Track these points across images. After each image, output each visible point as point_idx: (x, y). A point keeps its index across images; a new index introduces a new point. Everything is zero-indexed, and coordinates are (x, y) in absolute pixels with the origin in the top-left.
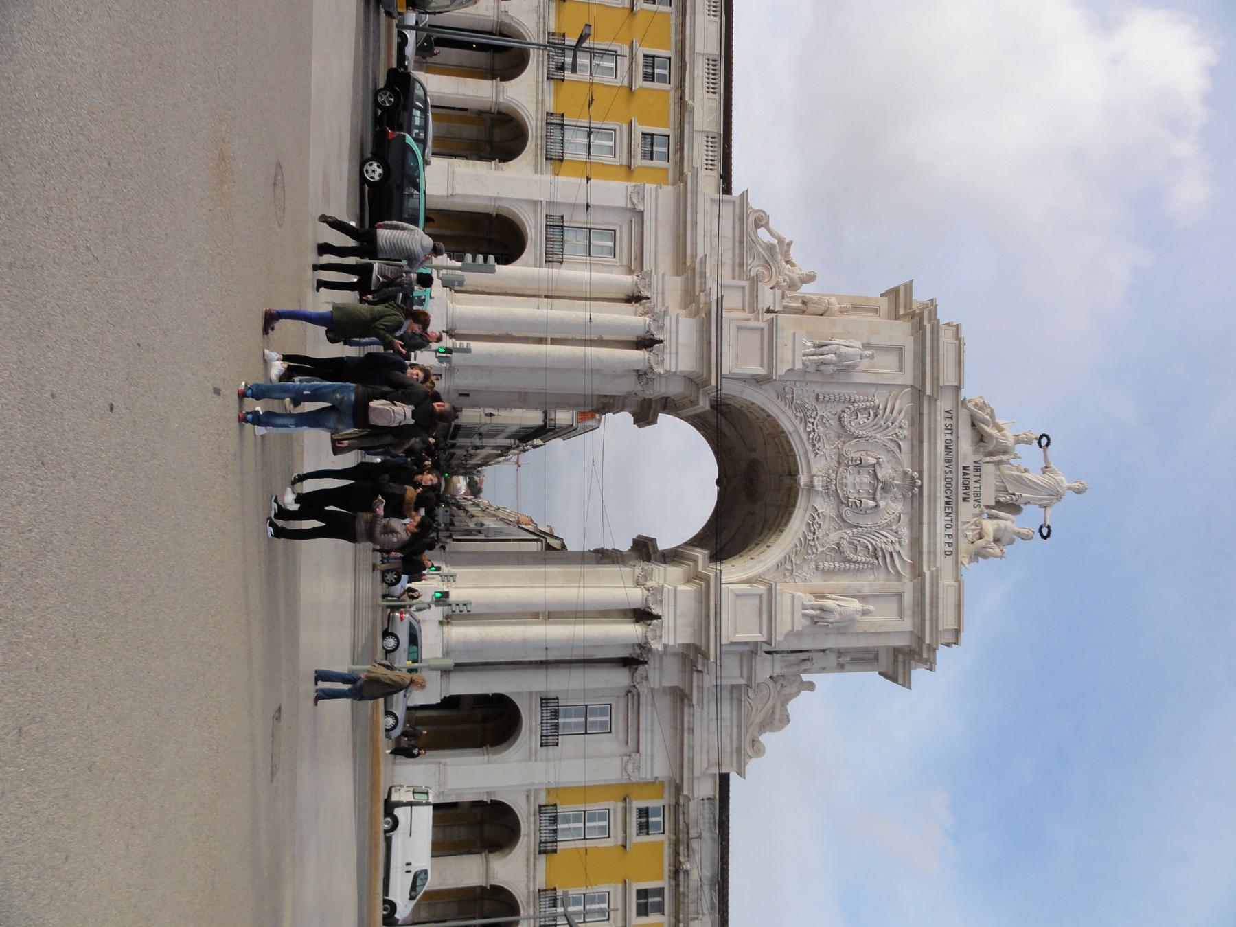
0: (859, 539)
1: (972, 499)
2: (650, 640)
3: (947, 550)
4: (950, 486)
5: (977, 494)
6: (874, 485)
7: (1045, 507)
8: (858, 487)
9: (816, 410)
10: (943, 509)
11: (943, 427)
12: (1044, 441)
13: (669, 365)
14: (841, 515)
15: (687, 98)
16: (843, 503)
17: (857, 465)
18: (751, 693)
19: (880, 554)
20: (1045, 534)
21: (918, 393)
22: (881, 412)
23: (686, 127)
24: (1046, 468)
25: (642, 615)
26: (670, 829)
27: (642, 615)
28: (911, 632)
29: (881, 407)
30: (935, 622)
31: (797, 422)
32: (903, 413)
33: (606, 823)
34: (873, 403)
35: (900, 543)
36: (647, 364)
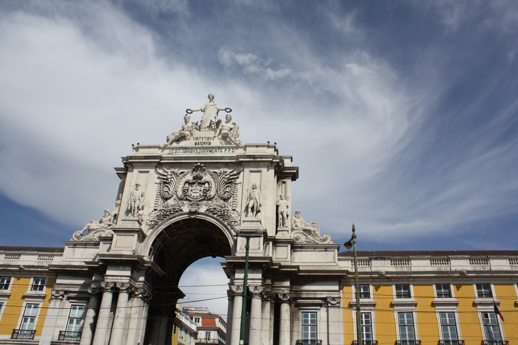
0: (223, 190)
2: (259, 292)
3: (232, 152)
4: (203, 150)
5: (208, 138)
6: (198, 184)
7: (219, 111)
9: (161, 210)
10: (213, 153)
11: (176, 153)
12: (189, 111)
13: (126, 280)
16: (205, 198)
17: (188, 191)
18: (299, 242)
19: (230, 181)
20: (229, 110)
21: (159, 165)
22: (165, 181)
24: (201, 110)
28: (268, 167)
29: (163, 181)
31: (165, 219)
32: (167, 170)
34: (161, 185)
35: (226, 172)
36: (125, 291)
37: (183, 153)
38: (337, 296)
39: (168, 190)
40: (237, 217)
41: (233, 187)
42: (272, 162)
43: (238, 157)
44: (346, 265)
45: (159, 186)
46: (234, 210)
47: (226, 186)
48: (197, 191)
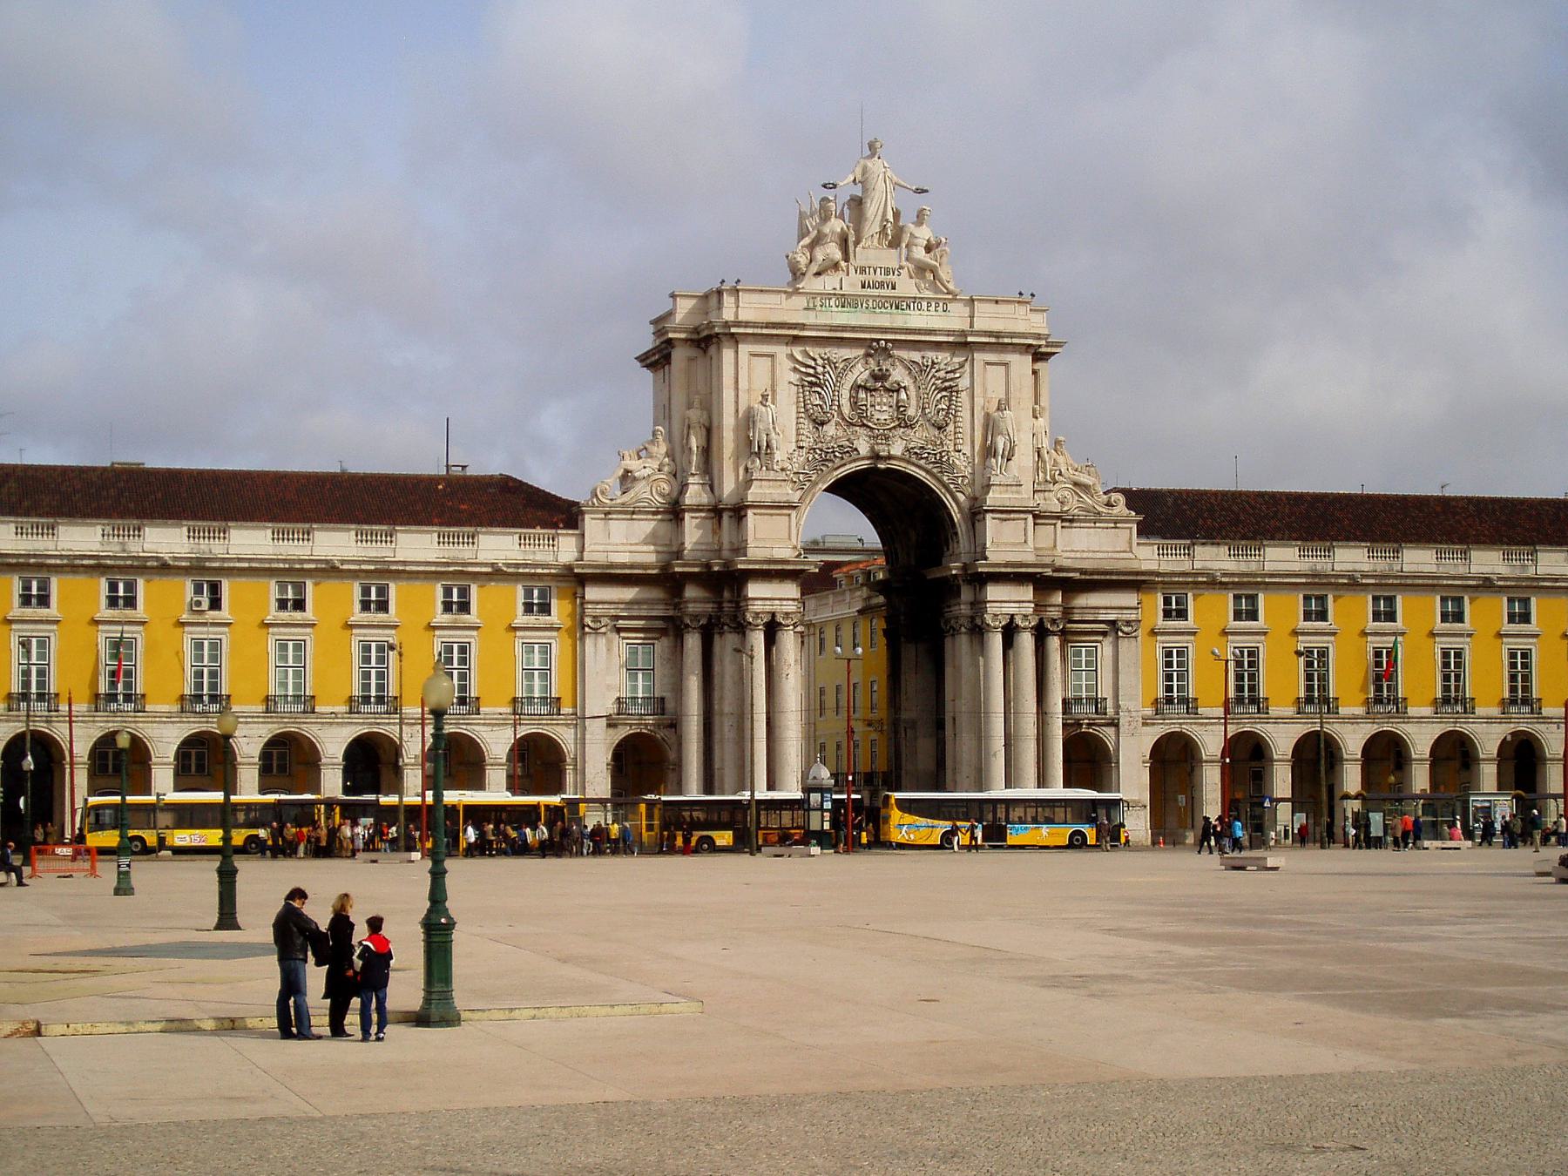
1: (893, 278)
5: (887, 271)
8: (885, 408)
9: (814, 449)
11: (824, 308)
14: (911, 425)
15: (489, 570)
19: (947, 384)
21: (796, 340)
22: (814, 379)
23: (521, 571)
25: (1010, 632)
26: (1183, 588)
27: (1010, 632)
29: (809, 379)
30: (1012, 335)
31: (824, 468)
33: (1175, 650)
34: (805, 389)
37: (837, 307)
38: (1133, 617)
39: (821, 403)
40: (966, 467)
41: (954, 398)
42: (1030, 346)
43: (963, 333)
44: (1148, 557)
45: (801, 390)
46: (959, 451)
47: (939, 395)
48: (885, 408)
